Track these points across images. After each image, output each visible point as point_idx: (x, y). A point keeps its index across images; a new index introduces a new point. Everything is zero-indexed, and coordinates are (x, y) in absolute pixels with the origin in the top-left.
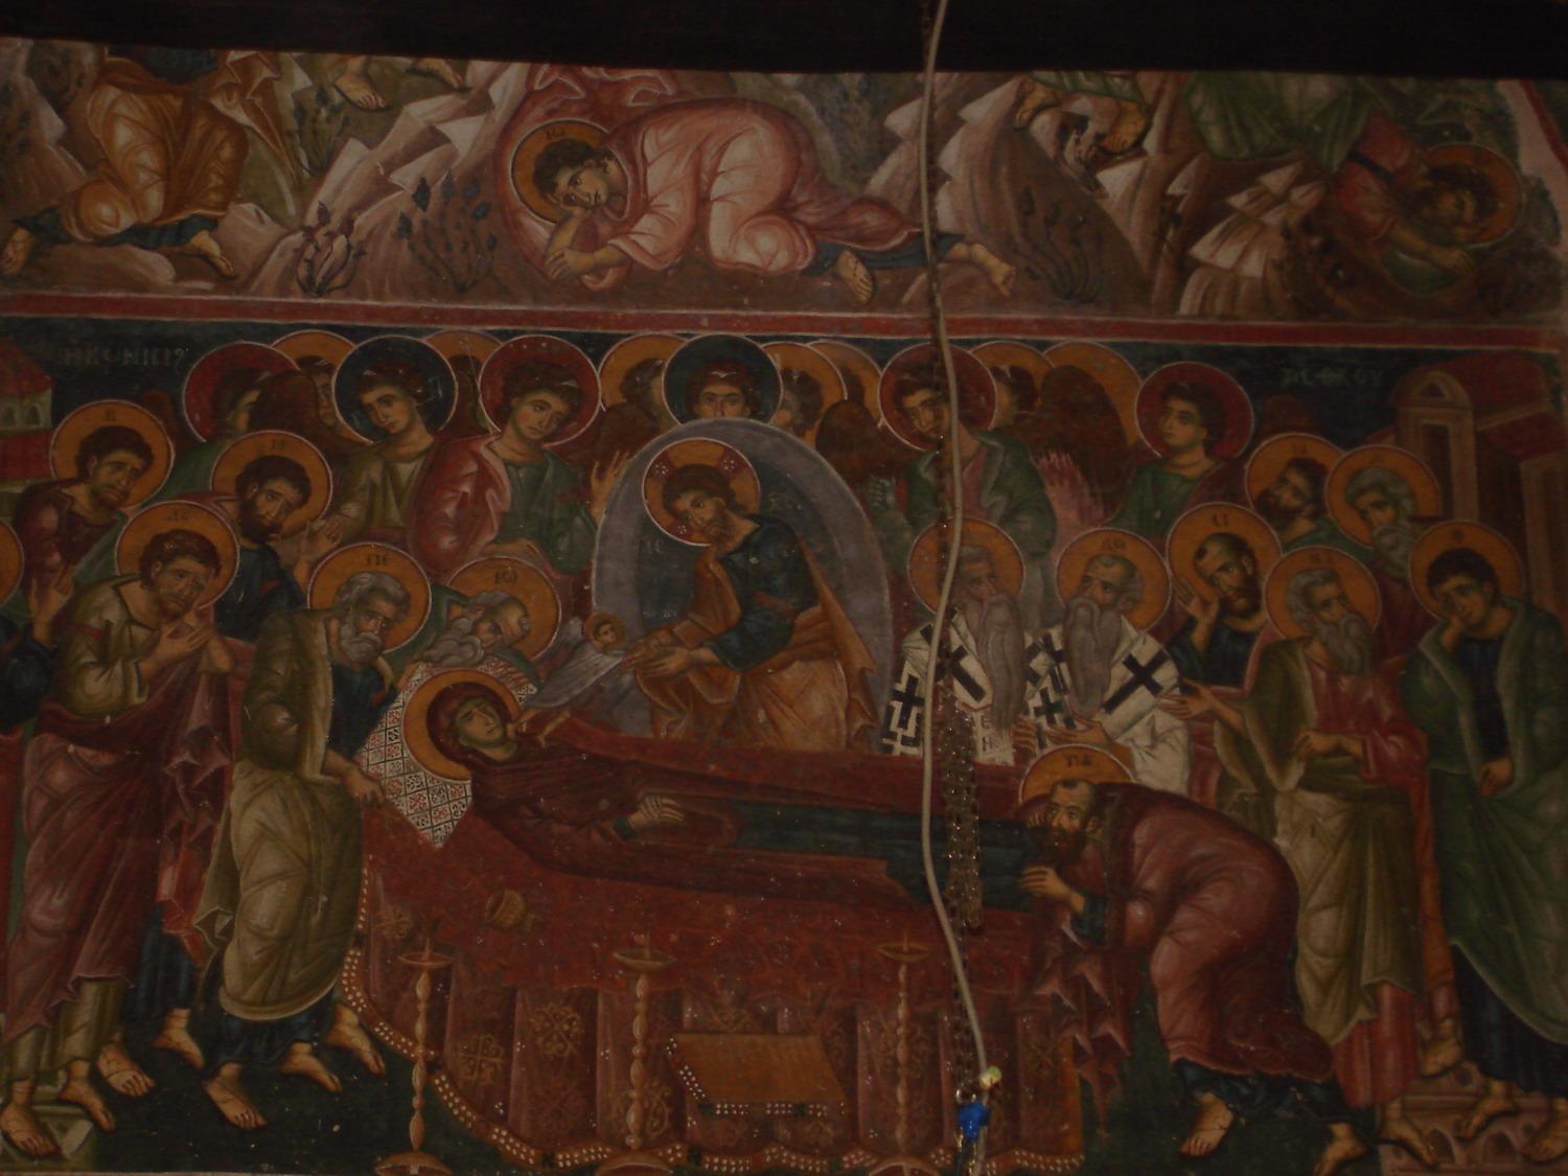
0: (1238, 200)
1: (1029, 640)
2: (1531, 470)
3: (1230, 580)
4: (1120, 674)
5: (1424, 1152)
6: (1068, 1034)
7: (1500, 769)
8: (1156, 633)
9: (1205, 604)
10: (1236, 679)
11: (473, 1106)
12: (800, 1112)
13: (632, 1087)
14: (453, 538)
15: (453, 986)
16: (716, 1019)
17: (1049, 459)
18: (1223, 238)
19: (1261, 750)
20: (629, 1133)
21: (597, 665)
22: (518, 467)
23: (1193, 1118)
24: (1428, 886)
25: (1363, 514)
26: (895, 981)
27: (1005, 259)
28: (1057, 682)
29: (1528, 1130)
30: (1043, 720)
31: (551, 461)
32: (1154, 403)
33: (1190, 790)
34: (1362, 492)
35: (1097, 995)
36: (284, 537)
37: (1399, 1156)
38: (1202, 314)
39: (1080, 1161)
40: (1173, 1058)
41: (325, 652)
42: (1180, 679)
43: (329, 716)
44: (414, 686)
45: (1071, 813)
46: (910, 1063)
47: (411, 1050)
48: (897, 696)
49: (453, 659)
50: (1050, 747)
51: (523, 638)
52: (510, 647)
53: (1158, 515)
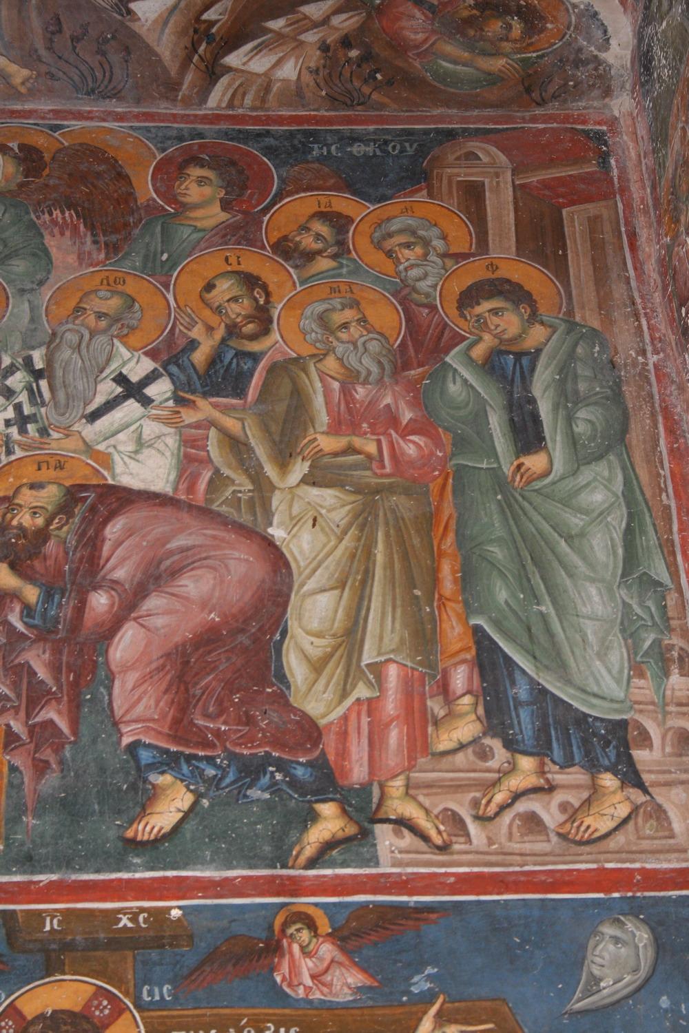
0: (277, 24)
1: (7, 361)
2: (575, 219)
3: (238, 311)
4: (108, 389)
5: (433, 833)
7: (535, 462)
8: (153, 354)
9: (210, 329)
10: (240, 392)
17: (51, 214)
18: (258, 50)
19: (261, 452)
23: (145, 799)
24: (447, 570)
25: (389, 254)
27: (25, 66)
28: (35, 395)
29: (564, 807)
30: (14, 431)
32: (171, 171)
33: (176, 489)
34: (390, 235)
35: (42, 682)
37: (398, 834)
38: (231, 105)
40: (126, 740)
42: (174, 392)
45: (34, 512)
50: (19, 453)
53: (165, 257)
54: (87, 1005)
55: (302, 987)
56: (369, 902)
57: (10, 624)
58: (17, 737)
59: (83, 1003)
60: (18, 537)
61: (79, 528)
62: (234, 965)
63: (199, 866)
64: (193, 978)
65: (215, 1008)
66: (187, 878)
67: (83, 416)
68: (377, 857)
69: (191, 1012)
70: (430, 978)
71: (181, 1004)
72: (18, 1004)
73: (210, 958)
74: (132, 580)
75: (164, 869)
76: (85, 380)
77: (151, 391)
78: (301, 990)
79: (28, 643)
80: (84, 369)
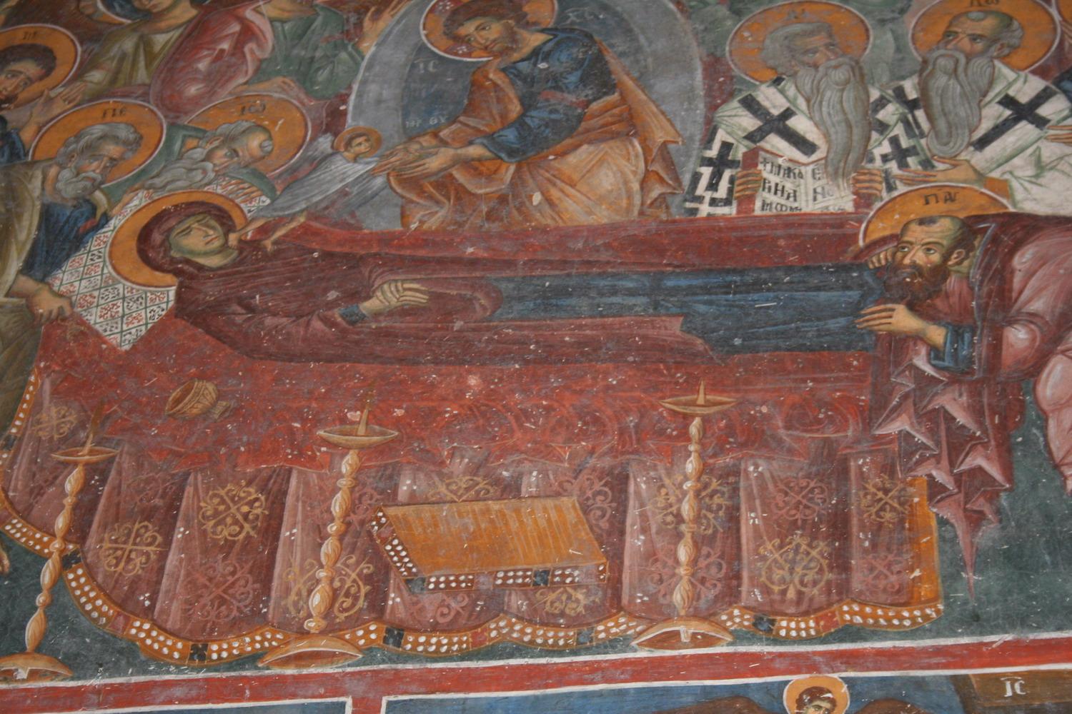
1: (875, 94)
4: (993, 113)
6: (921, 472)
8: (1042, 72)
11: (109, 598)
12: (544, 579)
13: (321, 566)
14: (201, 86)
15: (113, 474)
16: (443, 489)
20: (310, 616)
21: (344, 173)
22: (283, 22)
26: (684, 436)
30: (893, 166)
31: (321, 13)
35: (963, 427)
36: (17, 106)
39: (938, 611)
41: (37, 193)
43: (28, 247)
44: (130, 211)
46: (698, 519)
47: (47, 545)
48: (708, 162)
49: (179, 184)
50: (901, 189)
51: (263, 158)
52: (246, 167)
57: (917, 368)
58: (943, 488)
60: (913, 276)
61: (982, 261)
67: (970, 144)
74: (1052, 312)
76: (967, 105)
77: (1045, 110)
79: (940, 386)
80: (964, 95)
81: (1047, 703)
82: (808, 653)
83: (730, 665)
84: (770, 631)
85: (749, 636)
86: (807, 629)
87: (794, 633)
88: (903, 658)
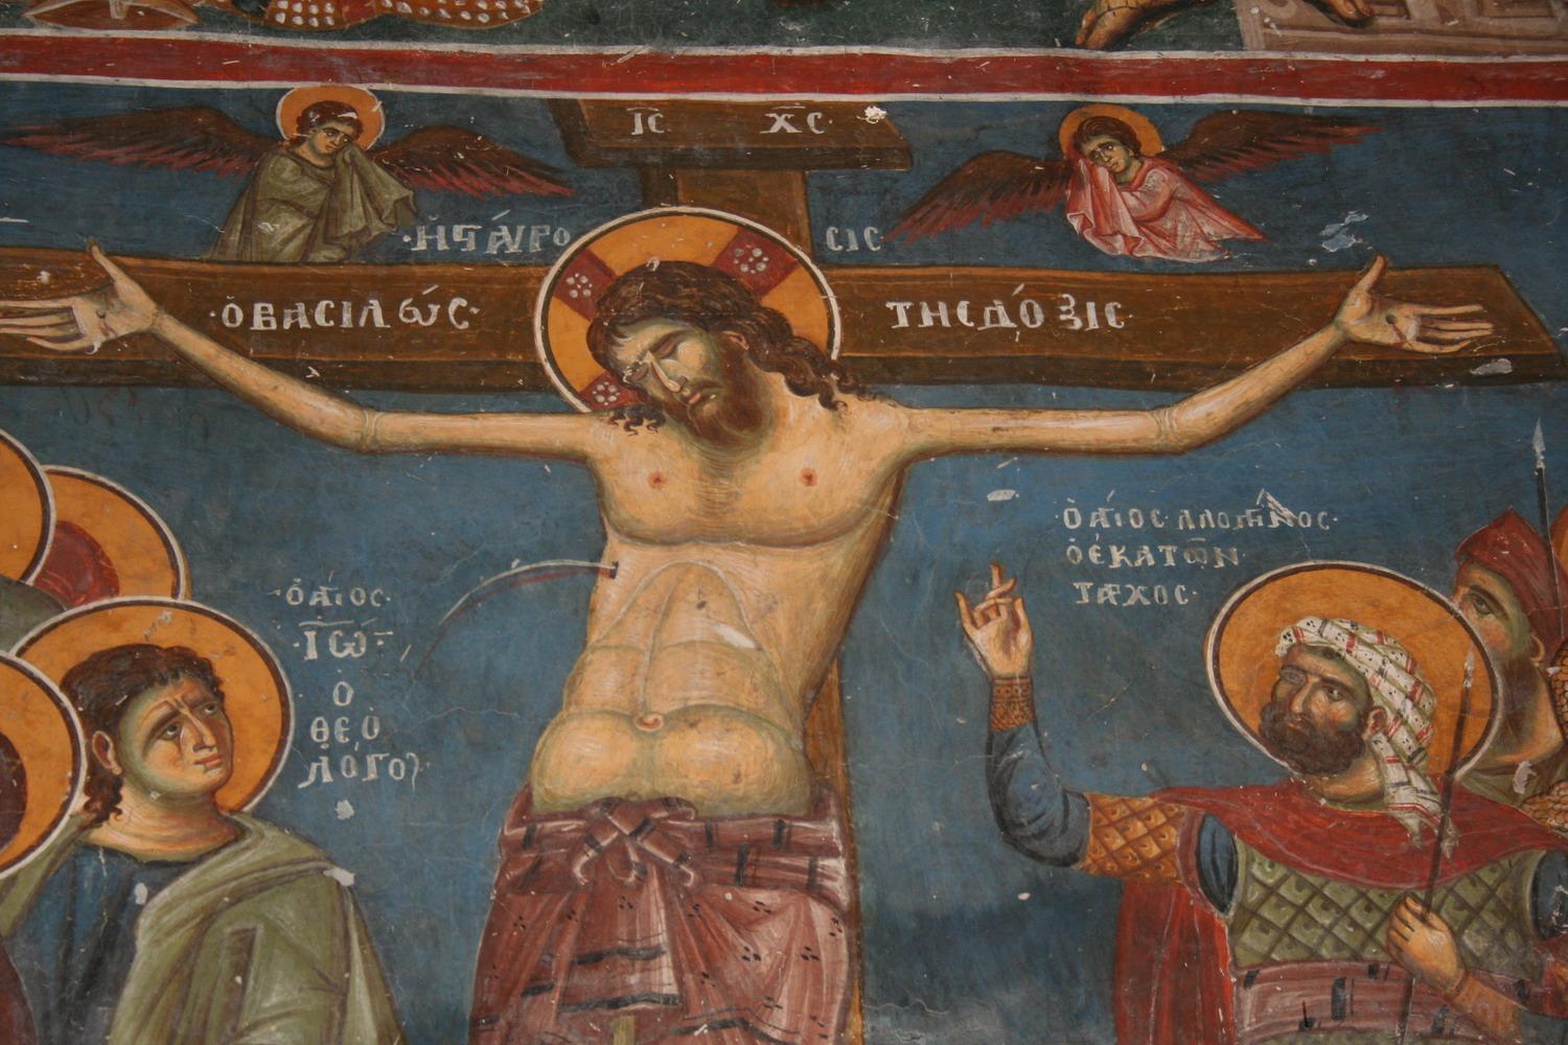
54: (725, 255)
55: (1120, 237)
56: (1229, 106)
59: (717, 252)
62: (992, 199)
63: (910, 40)
64: (918, 216)
65: (964, 265)
66: (890, 57)
68: (1238, 34)
69: (919, 272)
70: (1353, 229)
71: (899, 259)
72: (595, 249)
73: (945, 185)
75: (845, 42)
78: (1119, 242)
81: (696, 147)
82: (320, 50)
83: (188, 58)
84: (259, 14)
85: (224, 18)
86: (321, 16)
87: (299, 21)
88: (473, 69)
